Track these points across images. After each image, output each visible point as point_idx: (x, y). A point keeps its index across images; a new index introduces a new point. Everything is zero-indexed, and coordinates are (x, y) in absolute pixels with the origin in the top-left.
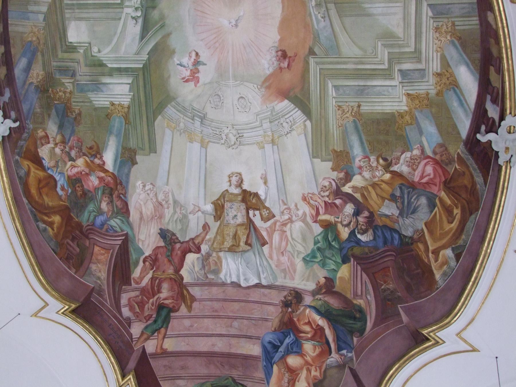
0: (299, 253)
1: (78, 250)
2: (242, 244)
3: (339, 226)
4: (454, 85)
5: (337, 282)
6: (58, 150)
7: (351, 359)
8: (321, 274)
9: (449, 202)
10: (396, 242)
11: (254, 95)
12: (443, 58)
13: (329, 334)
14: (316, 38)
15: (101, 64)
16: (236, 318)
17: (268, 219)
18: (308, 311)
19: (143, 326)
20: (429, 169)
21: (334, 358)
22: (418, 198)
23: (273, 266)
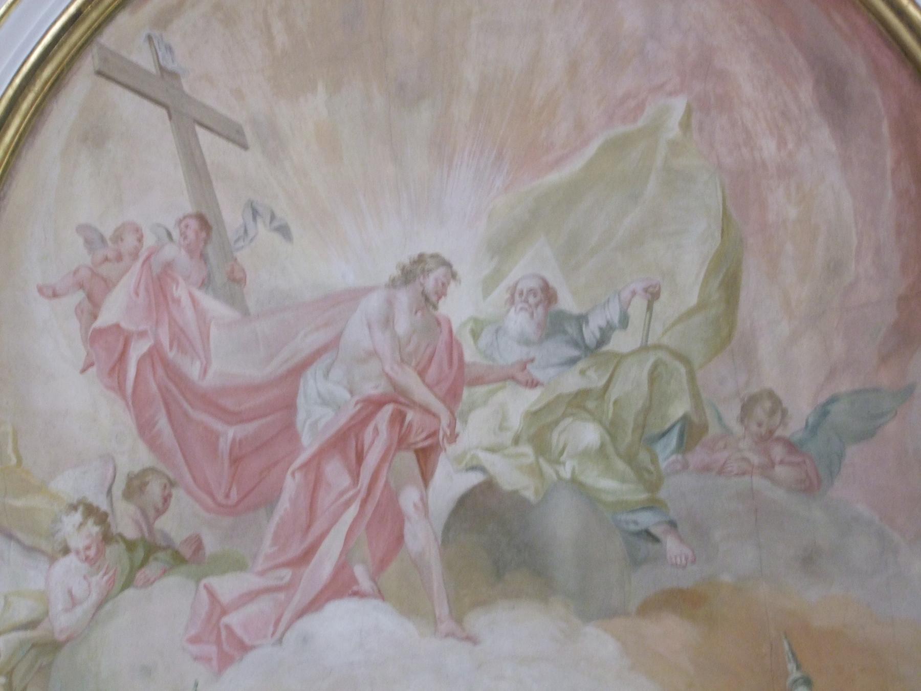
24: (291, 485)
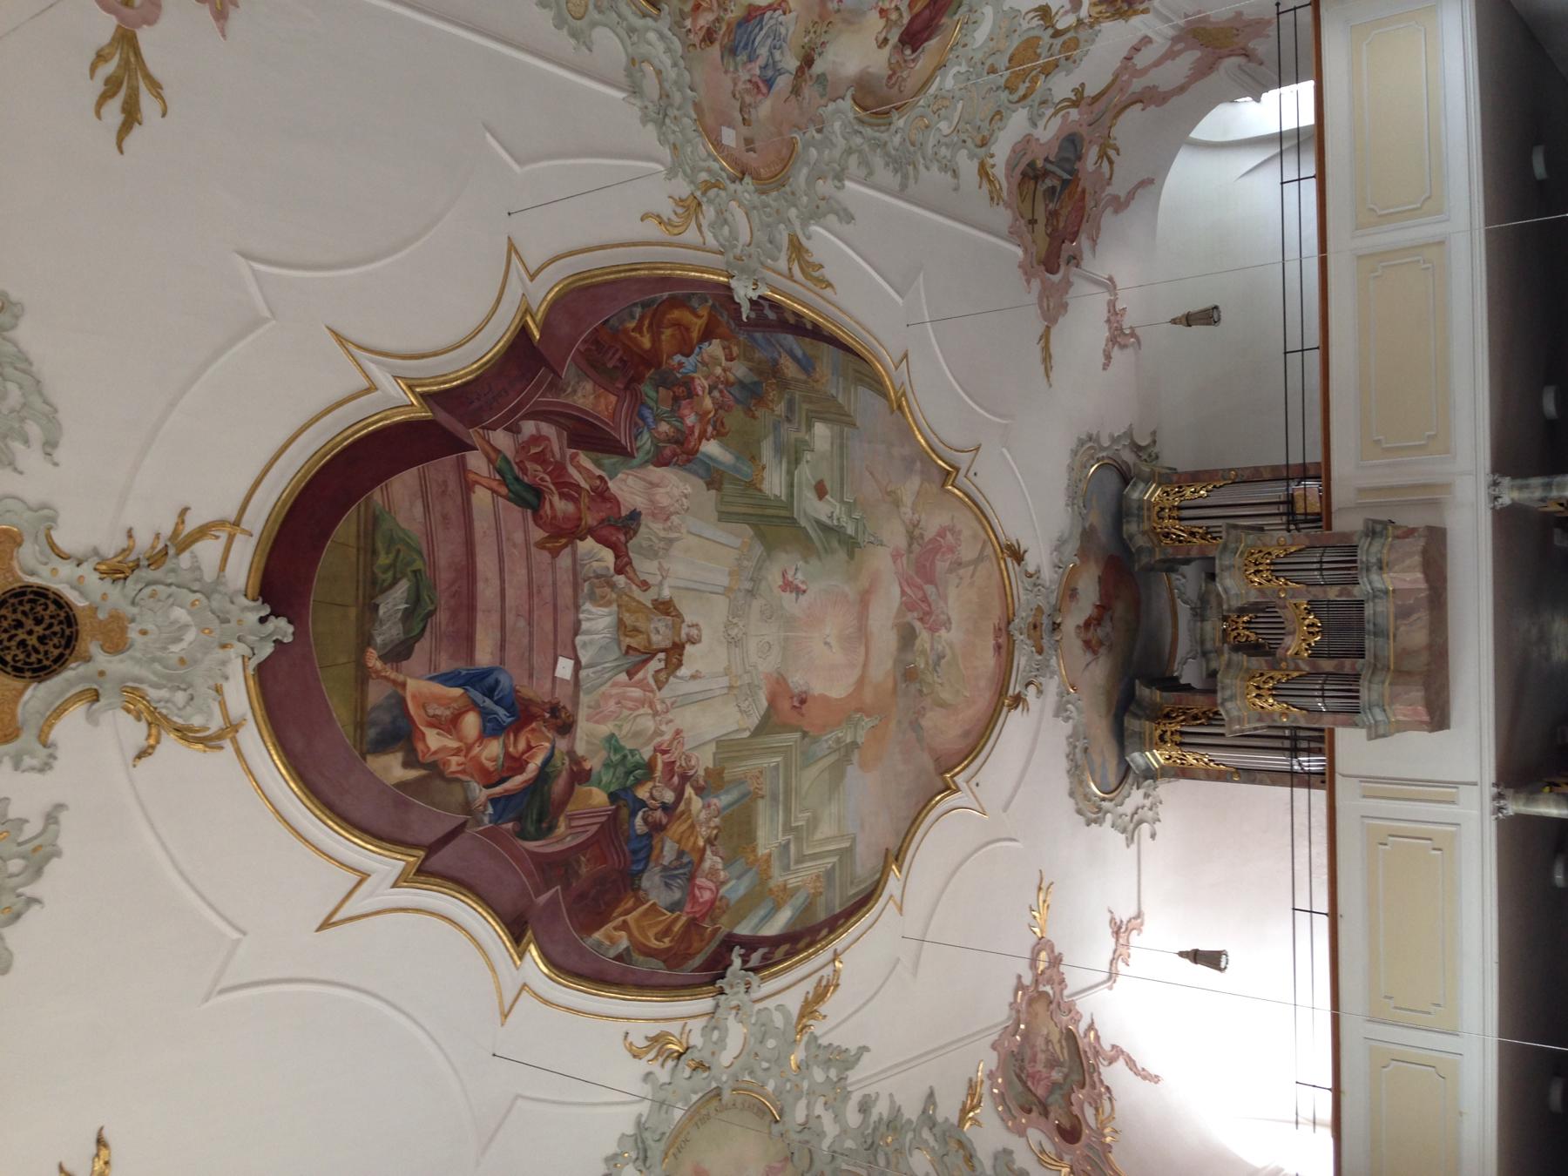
0: (620, 727)
1: (610, 365)
2: (628, 641)
3: (650, 785)
4: (777, 908)
5: (585, 788)
6: (718, 371)
7: (479, 823)
8: (594, 763)
9: (676, 929)
10: (635, 868)
11: (767, 665)
12: (797, 889)
13: (516, 782)
14: (815, 740)
15: (797, 461)
16: (530, 624)
17: (656, 681)
18: (547, 745)
19: (510, 455)
20: (707, 895)
21: (480, 794)
22: (680, 887)
23: (603, 689)
24: (919, 581)
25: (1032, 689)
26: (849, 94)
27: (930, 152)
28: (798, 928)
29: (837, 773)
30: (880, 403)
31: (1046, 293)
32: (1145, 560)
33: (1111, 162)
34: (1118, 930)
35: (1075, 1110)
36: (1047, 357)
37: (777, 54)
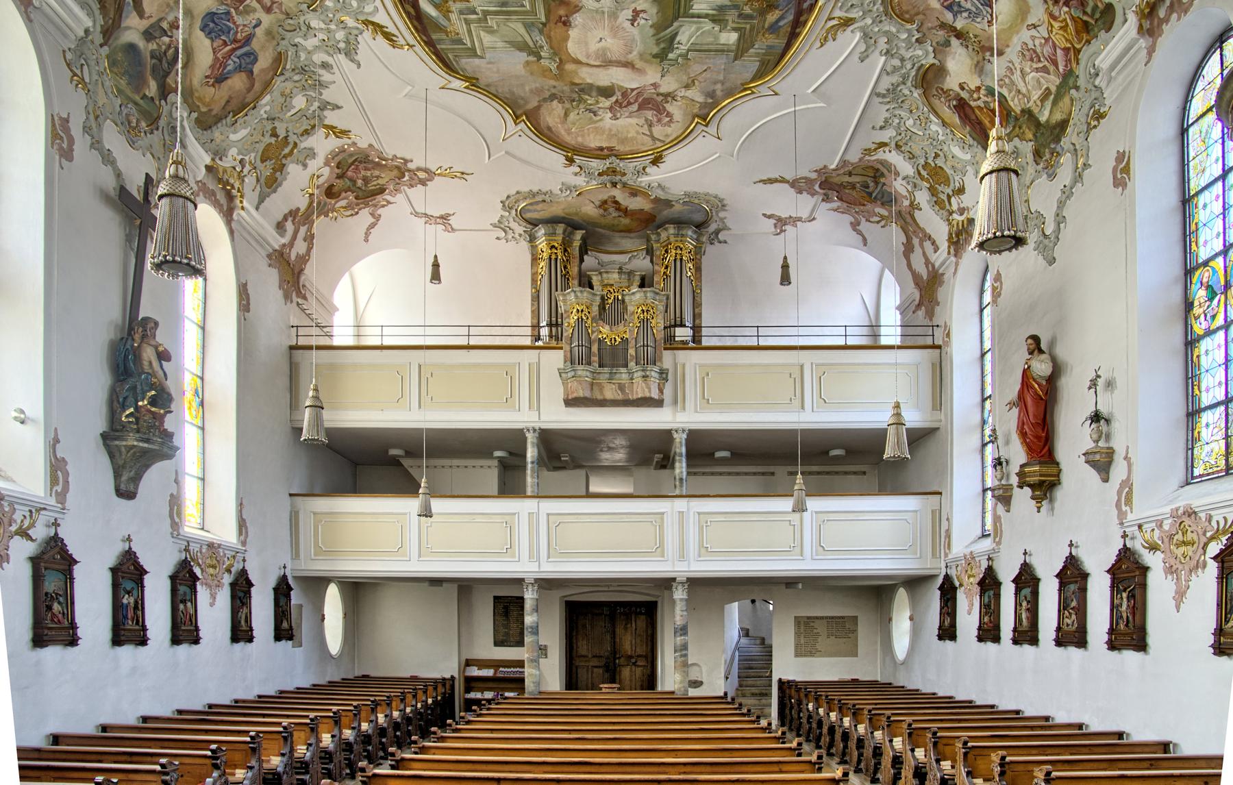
4: (436, 6)
12: (449, 20)
14: (541, 32)
15: (714, 21)
25: (578, 169)
26: (936, 62)
27: (897, 112)
28: (425, 21)
29: (522, 47)
30: (749, 76)
31: (809, 182)
32: (653, 237)
33: (878, 222)
34: (444, 218)
35: (343, 194)
36: (771, 181)
37: (965, 14)
